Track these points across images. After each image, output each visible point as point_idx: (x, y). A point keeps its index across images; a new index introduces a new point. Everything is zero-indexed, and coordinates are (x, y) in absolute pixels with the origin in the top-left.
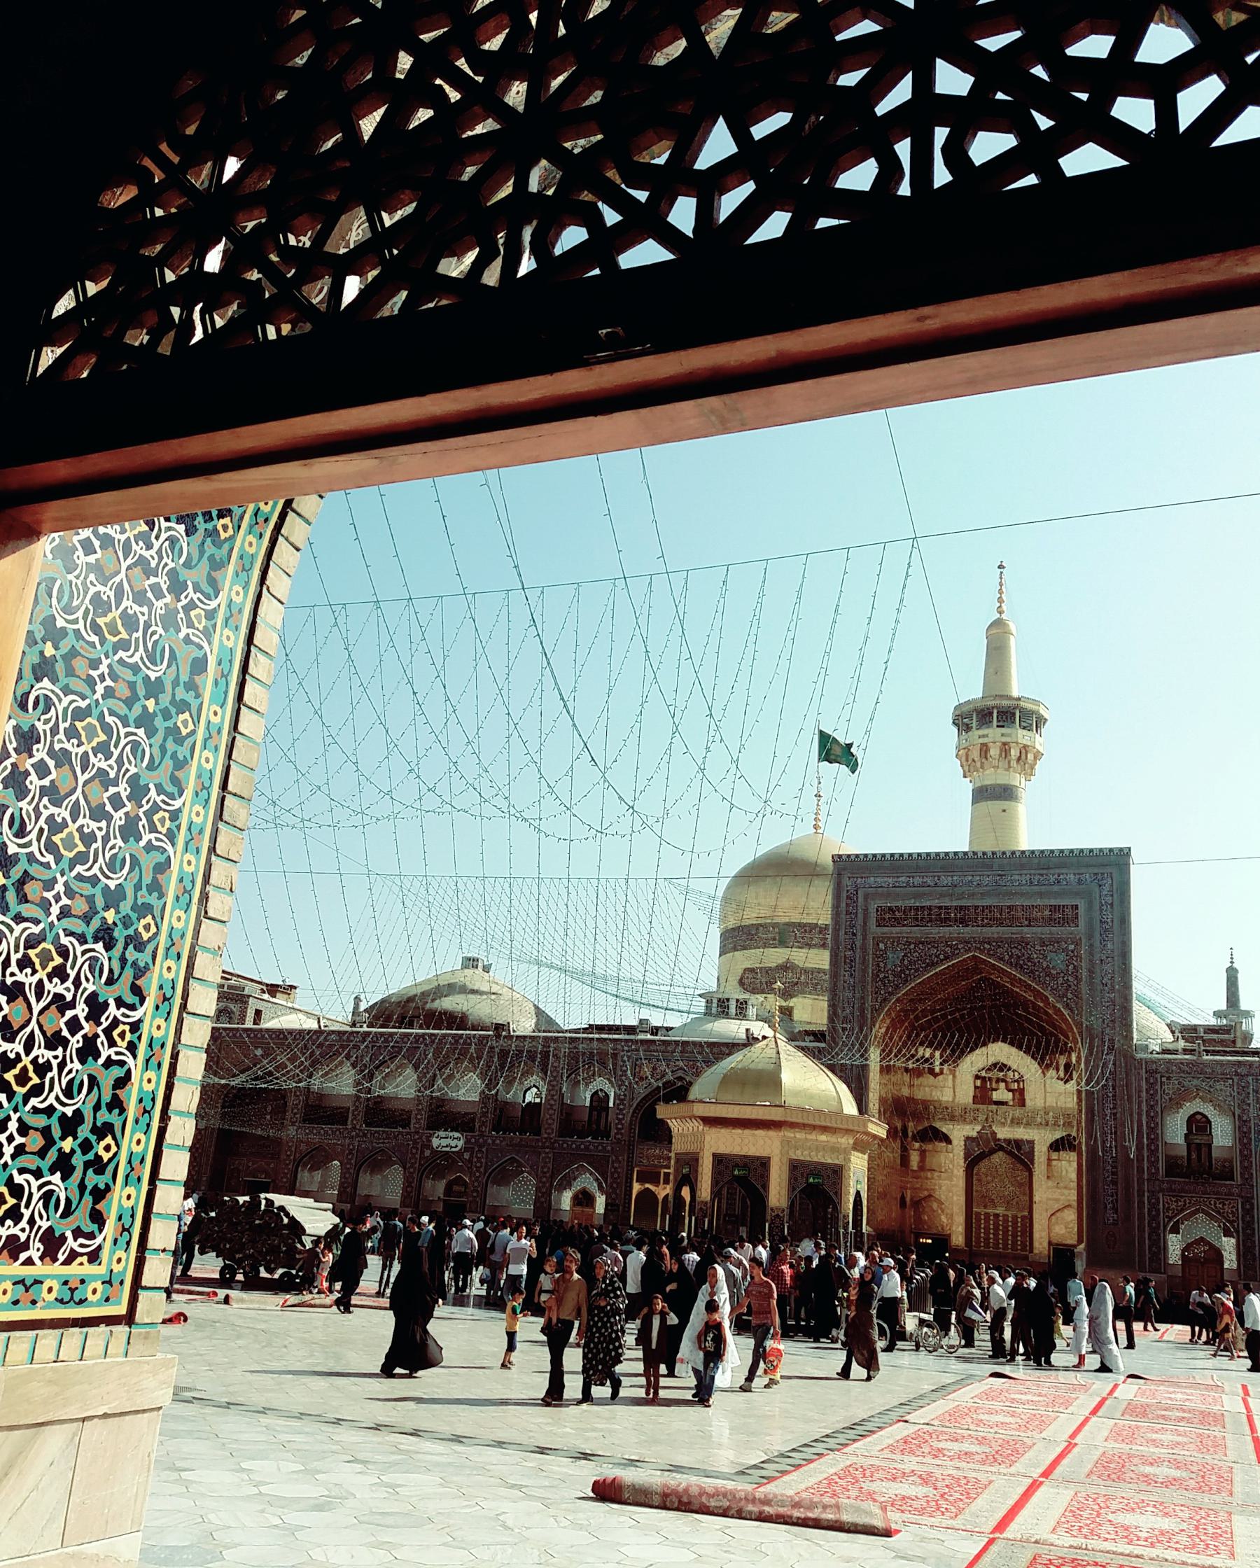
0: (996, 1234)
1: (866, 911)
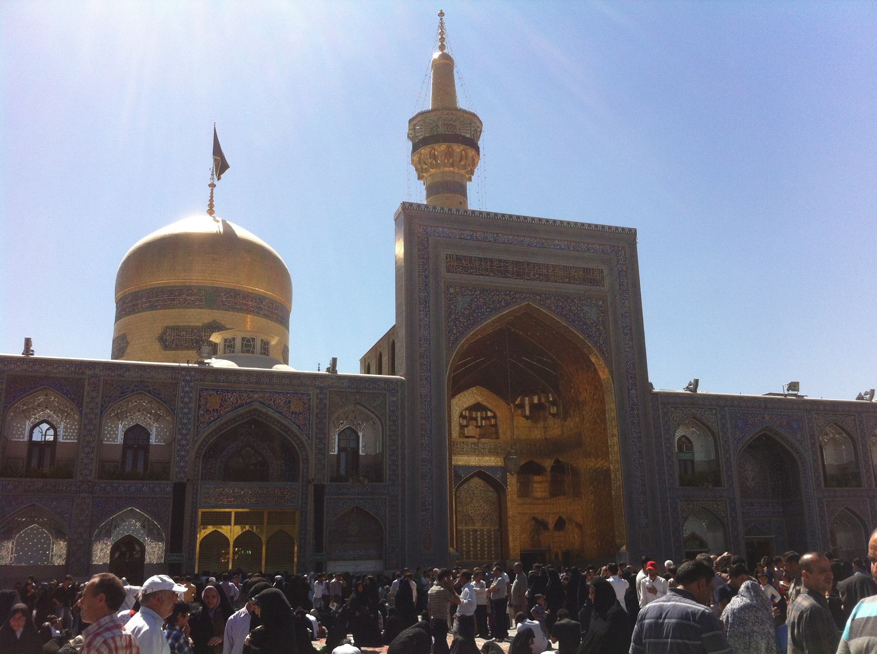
0: (475, 547)
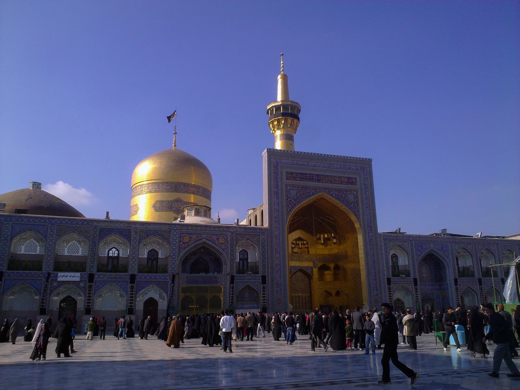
1: (281, 173)
